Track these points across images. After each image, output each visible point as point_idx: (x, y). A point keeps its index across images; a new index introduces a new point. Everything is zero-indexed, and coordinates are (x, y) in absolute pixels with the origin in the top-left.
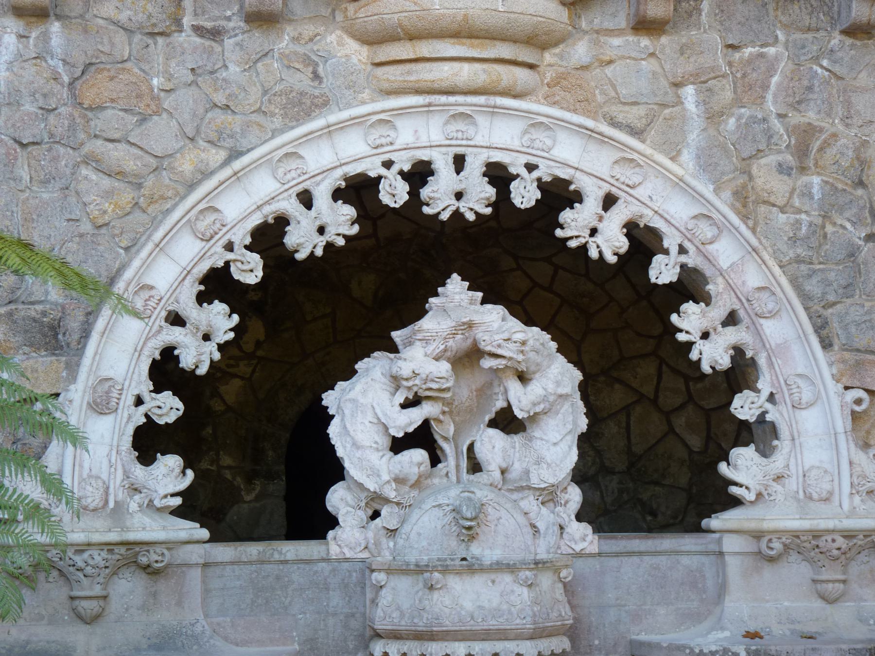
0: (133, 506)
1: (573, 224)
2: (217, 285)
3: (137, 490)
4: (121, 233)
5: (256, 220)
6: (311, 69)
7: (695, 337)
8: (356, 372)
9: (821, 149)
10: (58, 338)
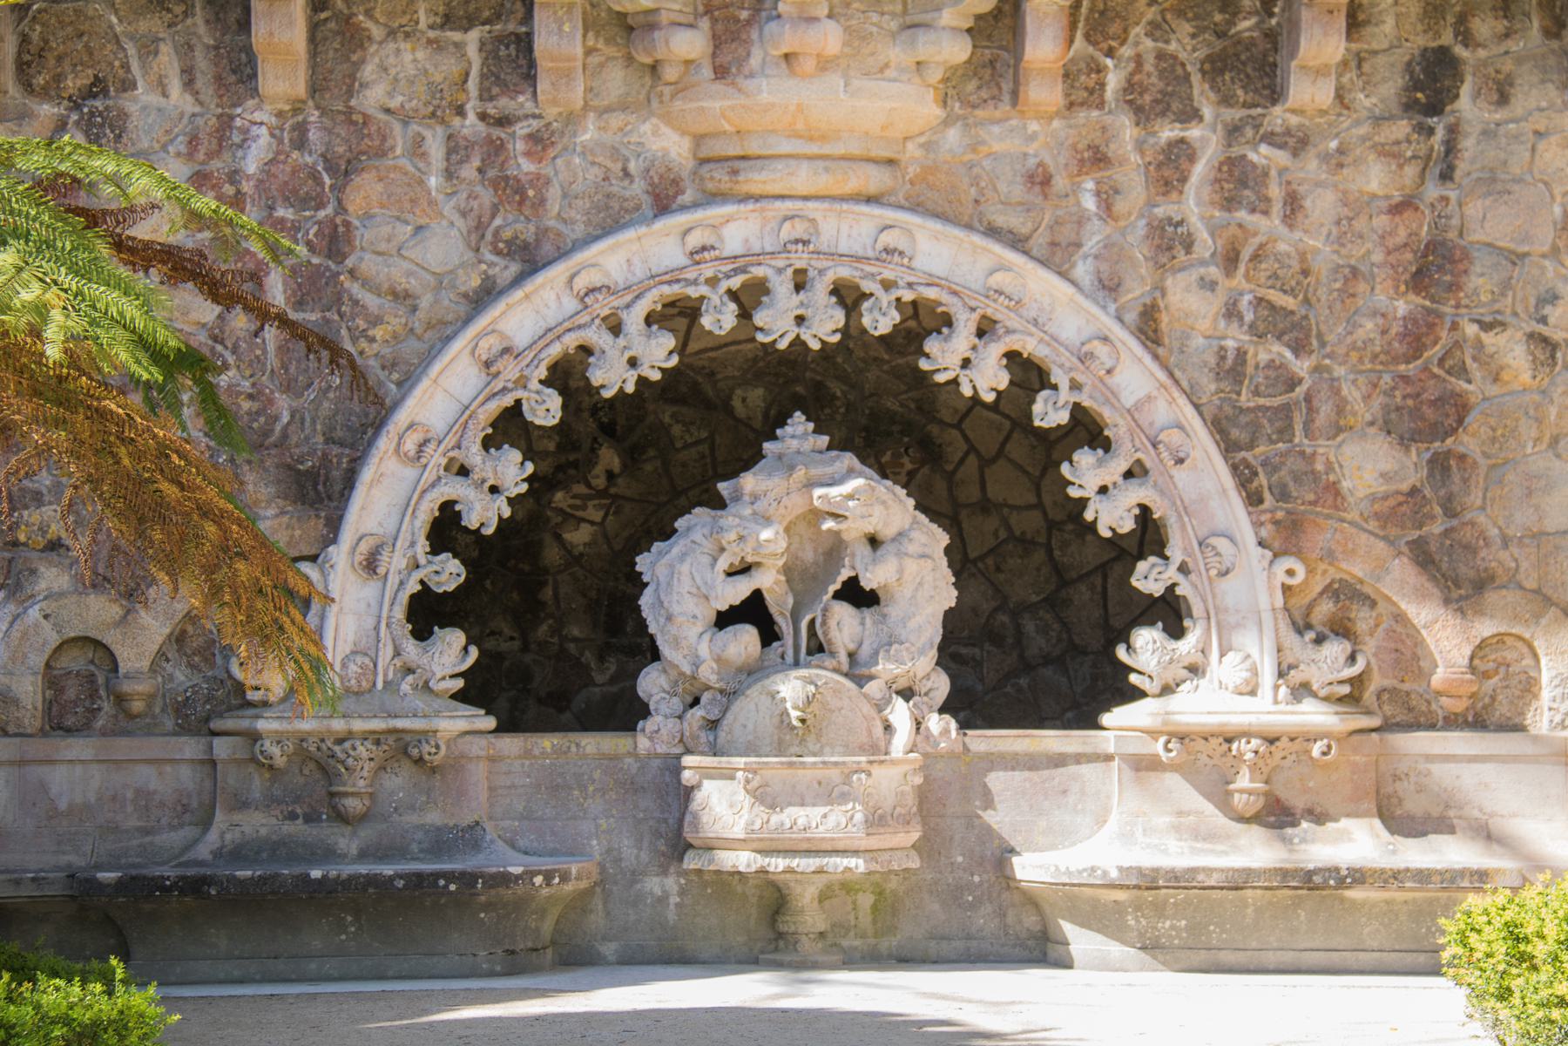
0: (405, 687)
2: (509, 427)
3: (410, 671)
4: (394, 365)
5: (555, 351)
6: (619, 165)
7: (1089, 491)
8: (676, 531)
9: (1256, 258)
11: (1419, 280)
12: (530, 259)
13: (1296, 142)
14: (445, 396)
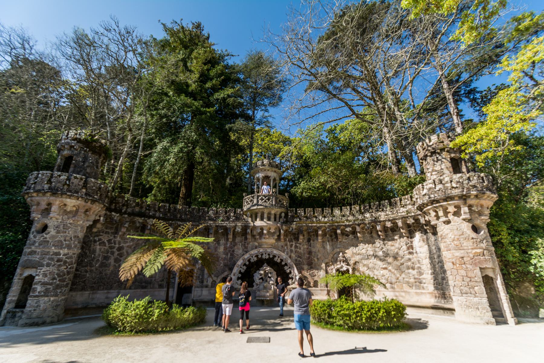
1: (276, 259)
10: (231, 269)
11: (309, 254)
12: (247, 252)
13: (300, 244)
14: (240, 262)
